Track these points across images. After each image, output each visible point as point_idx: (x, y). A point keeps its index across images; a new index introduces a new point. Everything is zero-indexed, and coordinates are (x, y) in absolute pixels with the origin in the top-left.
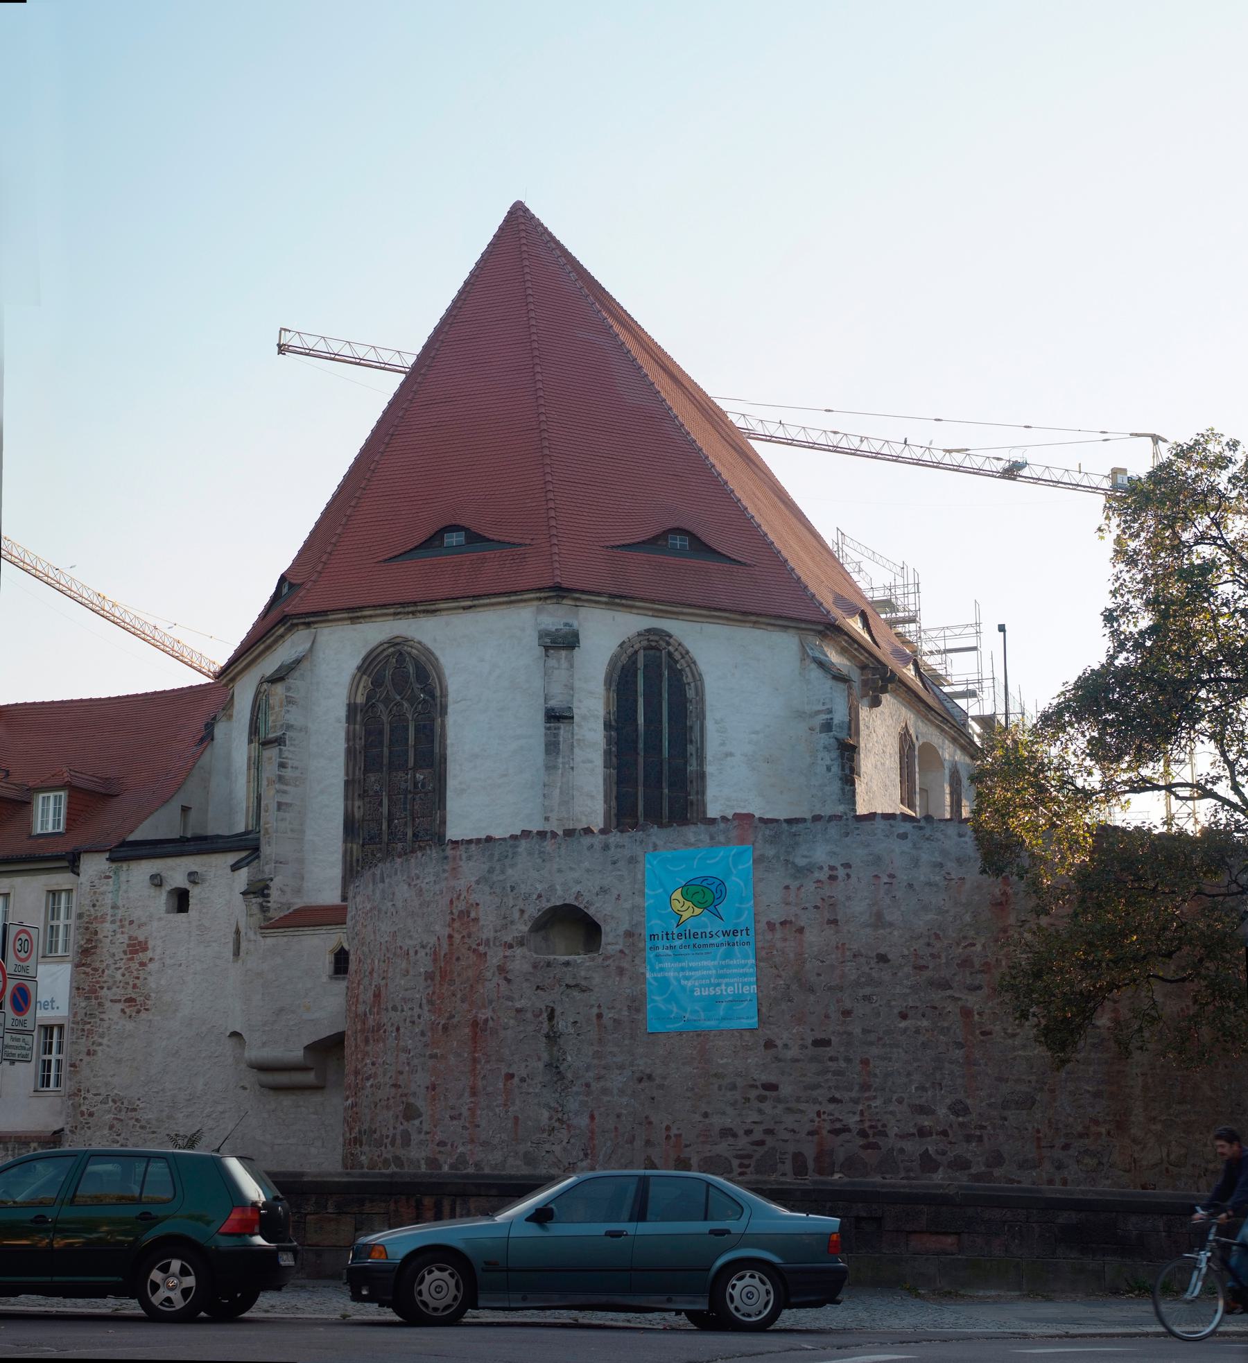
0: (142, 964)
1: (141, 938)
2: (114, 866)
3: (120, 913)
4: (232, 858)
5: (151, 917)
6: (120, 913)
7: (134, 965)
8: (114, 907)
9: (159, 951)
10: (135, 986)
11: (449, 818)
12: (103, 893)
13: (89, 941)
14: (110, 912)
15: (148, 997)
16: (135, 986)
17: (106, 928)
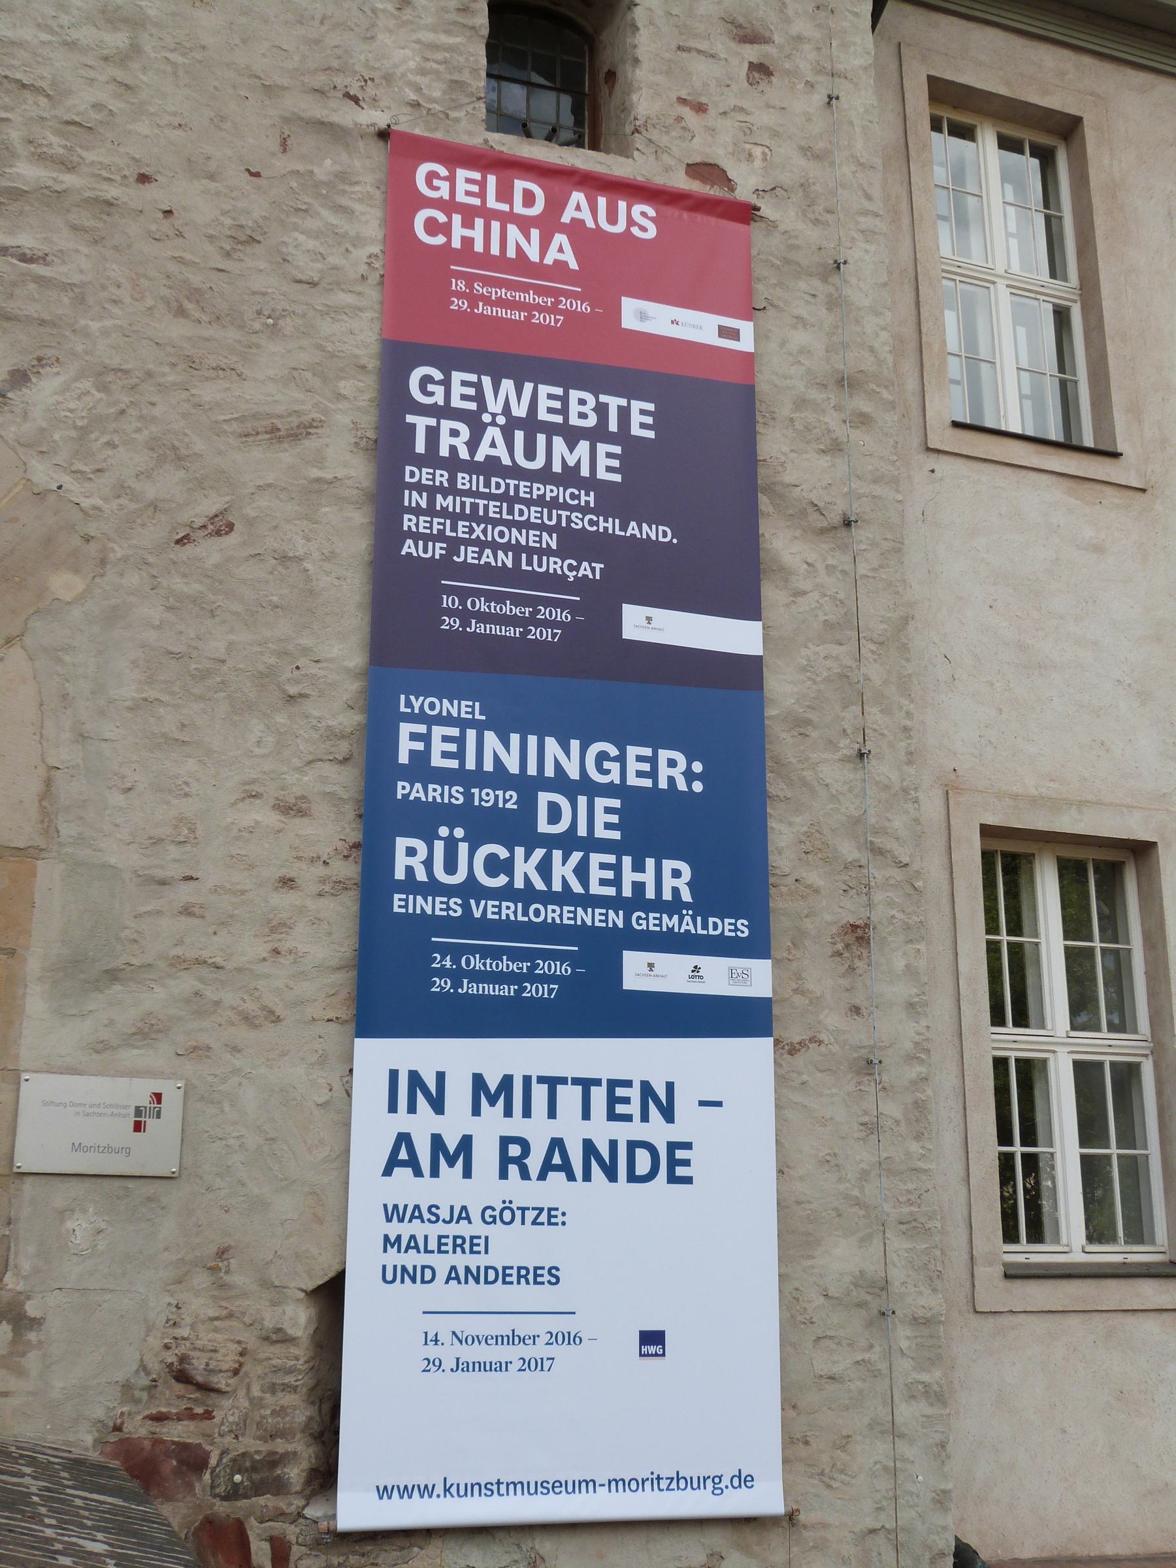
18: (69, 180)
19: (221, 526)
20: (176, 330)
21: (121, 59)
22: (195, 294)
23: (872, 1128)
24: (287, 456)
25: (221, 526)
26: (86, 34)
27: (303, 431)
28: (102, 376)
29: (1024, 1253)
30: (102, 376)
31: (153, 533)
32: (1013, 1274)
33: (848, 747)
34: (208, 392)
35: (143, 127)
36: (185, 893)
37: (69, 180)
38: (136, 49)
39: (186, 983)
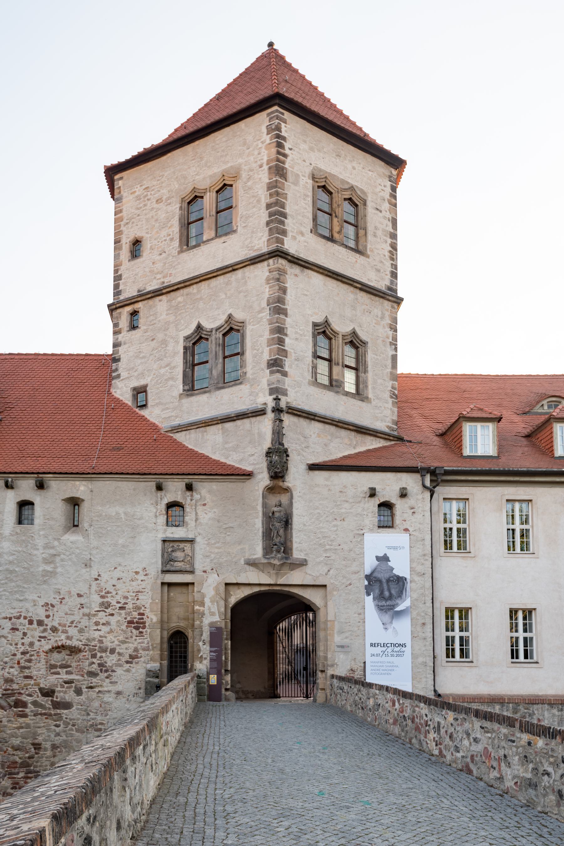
18: (332, 547)
19: (350, 584)
20: (344, 563)
21: (336, 531)
22: (346, 558)
23: (425, 646)
24: (357, 575)
25: (350, 584)
26: (332, 529)
27: (359, 572)
28: (337, 569)
29: (451, 659)
30: (337, 569)
31: (344, 586)
32: (447, 662)
33: (423, 602)
34: (348, 569)
35: (339, 539)
36: (349, 624)
37: (332, 547)
38: (337, 529)
39: (350, 633)
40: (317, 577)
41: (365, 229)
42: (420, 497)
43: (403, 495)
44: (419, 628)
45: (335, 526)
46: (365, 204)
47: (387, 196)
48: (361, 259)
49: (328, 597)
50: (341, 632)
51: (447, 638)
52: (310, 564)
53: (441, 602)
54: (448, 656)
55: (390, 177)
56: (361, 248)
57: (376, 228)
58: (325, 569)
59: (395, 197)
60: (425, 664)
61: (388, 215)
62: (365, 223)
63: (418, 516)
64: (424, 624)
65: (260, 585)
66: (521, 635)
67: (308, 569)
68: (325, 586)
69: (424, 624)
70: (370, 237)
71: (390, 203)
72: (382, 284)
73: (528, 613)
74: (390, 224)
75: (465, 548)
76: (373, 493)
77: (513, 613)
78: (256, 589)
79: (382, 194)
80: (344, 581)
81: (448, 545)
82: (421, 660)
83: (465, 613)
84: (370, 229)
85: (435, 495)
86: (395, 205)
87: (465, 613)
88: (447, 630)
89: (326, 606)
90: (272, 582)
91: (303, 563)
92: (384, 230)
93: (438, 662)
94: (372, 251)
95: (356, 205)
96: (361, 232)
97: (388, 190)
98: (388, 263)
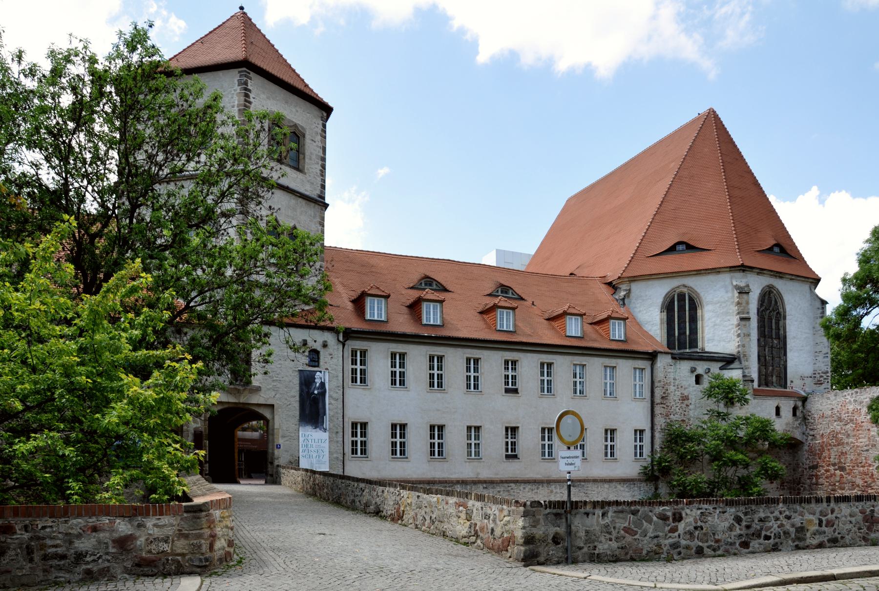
0: (687, 405)
1: (686, 394)
2: (674, 361)
3: (677, 382)
4: (720, 364)
5: (689, 385)
6: (677, 382)
7: (684, 406)
8: (674, 379)
9: (694, 400)
10: (684, 415)
11: (788, 359)
12: (669, 372)
13: (664, 393)
14: (673, 381)
15: (689, 420)
16: (684, 415)
17: (672, 388)
40: (268, 399)
41: (304, 154)
42: (336, 347)
43: (325, 345)
44: (334, 435)
45: (280, 364)
46: (304, 136)
47: (320, 131)
48: (300, 175)
49: (275, 413)
50: (283, 437)
51: (353, 441)
52: (263, 389)
53: (349, 418)
54: (353, 454)
55: (322, 117)
56: (300, 167)
57: (311, 153)
58: (273, 393)
59: (325, 132)
60: (337, 458)
61: (320, 144)
62: (304, 150)
63: (334, 360)
64: (337, 432)
65: (228, 403)
66: (398, 440)
67: (262, 394)
68: (273, 406)
69: (337, 432)
70: (307, 160)
71: (321, 136)
72: (313, 193)
73: (403, 427)
74: (321, 151)
75: (365, 383)
76: (305, 343)
77: (394, 426)
78: (226, 406)
79: (316, 129)
80: (286, 402)
81: (354, 380)
82: (335, 455)
83: (364, 425)
84: (307, 153)
85: (346, 346)
86: (325, 138)
87: (364, 425)
88: (353, 436)
89: (273, 418)
90: (237, 401)
91: (258, 389)
92: (317, 155)
93: (346, 457)
94: (308, 170)
95: (299, 137)
96: (301, 156)
97: (321, 127)
98: (319, 179)
